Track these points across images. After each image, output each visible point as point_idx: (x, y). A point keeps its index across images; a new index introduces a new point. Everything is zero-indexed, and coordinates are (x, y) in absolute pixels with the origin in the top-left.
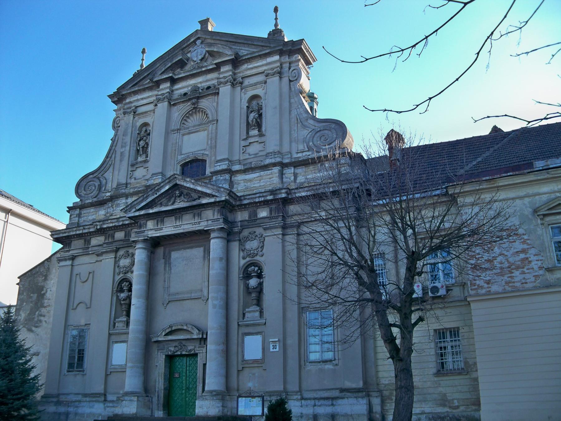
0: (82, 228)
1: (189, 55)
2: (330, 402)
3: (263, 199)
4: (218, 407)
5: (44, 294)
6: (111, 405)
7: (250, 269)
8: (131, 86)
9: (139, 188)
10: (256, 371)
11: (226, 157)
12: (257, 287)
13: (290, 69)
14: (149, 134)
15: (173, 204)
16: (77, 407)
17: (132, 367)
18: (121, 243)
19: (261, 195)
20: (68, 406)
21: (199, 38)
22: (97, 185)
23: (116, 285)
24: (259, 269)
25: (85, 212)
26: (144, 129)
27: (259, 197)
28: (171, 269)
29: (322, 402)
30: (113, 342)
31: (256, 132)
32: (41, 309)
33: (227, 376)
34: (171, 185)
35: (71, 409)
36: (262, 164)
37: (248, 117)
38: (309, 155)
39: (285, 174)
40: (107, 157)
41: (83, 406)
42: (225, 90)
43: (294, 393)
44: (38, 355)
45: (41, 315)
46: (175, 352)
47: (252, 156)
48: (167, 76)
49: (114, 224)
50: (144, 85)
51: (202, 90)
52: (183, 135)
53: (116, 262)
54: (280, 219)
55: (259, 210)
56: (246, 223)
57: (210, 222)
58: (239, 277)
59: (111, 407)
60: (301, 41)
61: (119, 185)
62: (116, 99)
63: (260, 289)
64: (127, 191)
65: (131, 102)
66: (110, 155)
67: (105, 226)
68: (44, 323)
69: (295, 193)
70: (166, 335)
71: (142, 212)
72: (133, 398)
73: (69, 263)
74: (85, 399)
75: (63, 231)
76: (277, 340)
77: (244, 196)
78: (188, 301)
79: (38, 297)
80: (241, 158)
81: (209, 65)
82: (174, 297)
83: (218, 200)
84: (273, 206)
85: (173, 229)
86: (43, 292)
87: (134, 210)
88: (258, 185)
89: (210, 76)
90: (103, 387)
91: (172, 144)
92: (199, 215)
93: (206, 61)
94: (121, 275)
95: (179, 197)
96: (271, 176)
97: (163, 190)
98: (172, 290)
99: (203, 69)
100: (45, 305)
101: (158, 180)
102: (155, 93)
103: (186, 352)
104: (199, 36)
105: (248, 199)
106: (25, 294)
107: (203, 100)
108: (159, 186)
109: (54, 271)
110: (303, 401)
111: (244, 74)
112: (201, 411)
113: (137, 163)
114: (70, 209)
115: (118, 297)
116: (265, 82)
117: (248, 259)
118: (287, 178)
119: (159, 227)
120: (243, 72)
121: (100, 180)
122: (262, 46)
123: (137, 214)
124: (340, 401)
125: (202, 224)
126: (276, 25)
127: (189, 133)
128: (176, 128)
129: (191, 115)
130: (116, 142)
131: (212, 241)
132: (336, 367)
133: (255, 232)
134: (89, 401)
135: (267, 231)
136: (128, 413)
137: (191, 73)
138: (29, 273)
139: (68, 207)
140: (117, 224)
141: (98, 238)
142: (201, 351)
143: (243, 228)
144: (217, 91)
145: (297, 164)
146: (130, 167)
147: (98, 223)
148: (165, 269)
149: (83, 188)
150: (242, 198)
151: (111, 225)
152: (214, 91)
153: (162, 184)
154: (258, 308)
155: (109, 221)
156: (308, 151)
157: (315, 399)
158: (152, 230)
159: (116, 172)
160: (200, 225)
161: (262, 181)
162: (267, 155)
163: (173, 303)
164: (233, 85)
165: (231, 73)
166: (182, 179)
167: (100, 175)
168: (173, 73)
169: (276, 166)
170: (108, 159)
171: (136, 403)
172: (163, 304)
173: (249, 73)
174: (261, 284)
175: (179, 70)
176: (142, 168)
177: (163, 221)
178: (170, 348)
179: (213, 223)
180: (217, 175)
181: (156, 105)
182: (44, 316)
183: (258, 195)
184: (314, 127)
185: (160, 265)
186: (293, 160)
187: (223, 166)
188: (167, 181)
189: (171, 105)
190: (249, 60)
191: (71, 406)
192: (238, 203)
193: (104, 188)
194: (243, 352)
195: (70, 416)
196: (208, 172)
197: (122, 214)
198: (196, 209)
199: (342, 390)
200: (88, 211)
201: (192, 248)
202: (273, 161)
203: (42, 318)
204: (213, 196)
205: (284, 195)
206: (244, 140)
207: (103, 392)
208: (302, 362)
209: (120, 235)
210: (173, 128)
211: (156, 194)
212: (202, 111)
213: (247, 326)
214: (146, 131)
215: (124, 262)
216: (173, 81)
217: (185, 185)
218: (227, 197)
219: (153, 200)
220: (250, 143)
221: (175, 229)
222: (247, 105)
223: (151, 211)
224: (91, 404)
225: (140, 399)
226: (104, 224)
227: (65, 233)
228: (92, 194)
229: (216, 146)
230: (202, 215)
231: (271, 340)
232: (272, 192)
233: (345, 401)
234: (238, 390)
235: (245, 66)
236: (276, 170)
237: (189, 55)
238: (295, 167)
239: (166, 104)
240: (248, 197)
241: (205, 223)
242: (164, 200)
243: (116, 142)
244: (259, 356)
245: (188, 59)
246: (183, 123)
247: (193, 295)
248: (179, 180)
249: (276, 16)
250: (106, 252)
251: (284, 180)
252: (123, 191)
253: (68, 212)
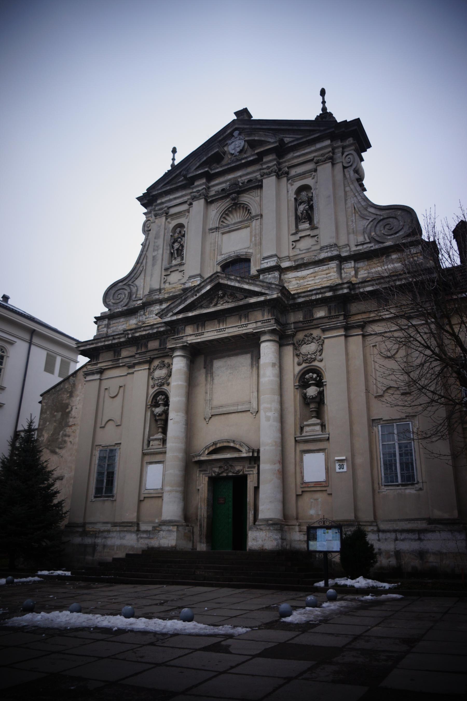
0: (111, 338)
1: (226, 149)
2: (416, 536)
3: (320, 296)
4: (276, 539)
5: (69, 412)
6: (145, 536)
7: (307, 376)
8: (161, 185)
9: (174, 292)
10: (318, 495)
11: (274, 253)
12: (316, 397)
13: (343, 154)
14: (184, 236)
15: (216, 305)
16: (105, 538)
17: (170, 491)
18: (156, 352)
19: (319, 291)
20: (96, 537)
21: (236, 129)
22: (126, 293)
23: (150, 399)
24: (318, 376)
25: (114, 322)
26: (178, 230)
27: (316, 294)
28: (213, 379)
29: (404, 535)
30: (147, 463)
31: (307, 225)
32: (65, 428)
33: (284, 502)
34: (213, 284)
35: (99, 541)
36: (317, 259)
37: (296, 210)
38: (371, 247)
39: (344, 269)
40: (137, 263)
41: (112, 537)
42: (270, 183)
43: (368, 524)
44: (62, 479)
45: (66, 435)
46: (220, 474)
47: (304, 251)
48: (202, 171)
49: (147, 332)
50: (176, 183)
51: (242, 183)
52: (223, 234)
53: (150, 374)
54: (341, 318)
55: (315, 310)
56: (300, 325)
57: (259, 324)
58: (295, 386)
59: (146, 538)
60: (357, 122)
61: (152, 291)
62: (146, 201)
63: (320, 400)
64: (161, 297)
65: (162, 203)
66: (141, 261)
67: (137, 335)
68: (69, 443)
69: (359, 288)
70: (210, 453)
71: (180, 316)
72: (171, 528)
73: (97, 377)
74: (114, 529)
75: (90, 342)
76: (344, 458)
77: (298, 294)
78: (233, 415)
79: (62, 415)
80: (291, 255)
81: (250, 157)
82: (218, 410)
83: (268, 297)
84: (333, 305)
85: (216, 334)
86: (67, 410)
87: (171, 314)
88: (313, 282)
89: (250, 169)
90: (135, 514)
91: (211, 244)
92: (246, 317)
93: (245, 153)
94: (156, 388)
95: (222, 298)
96: (327, 271)
97: (204, 291)
98: (216, 403)
99: (243, 161)
100: (70, 424)
101: (197, 281)
102: (190, 191)
103: (233, 473)
104: (236, 126)
105: (303, 297)
106: (48, 413)
107: (245, 195)
108: (200, 287)
110: (381, 534)
111: (290, 163)
112: (255, 544)
113: (171, 267)
114: (98, 320)
115: (152, 412)
116: (315, 170)
117: (304, 365)
118: (346, 273)
119: (200, 331)
120: (289, 160)
121: (130, 288)
122: (310, 131)
123: (175, 318)
124: (429, 535)
125: (250, 326)
126: (324, 109)
127: (229, 232)
128: (214, 226)
129: (231, 212)
130: (146, 247)
131: (263, 346)
132: (421, 492)
133: (311, 334)
134: (120, 531)
135: (326, 333)
136: (166, 545)
137: (229, 166)
138: (53, 390)
139: (95, 318)
140: (151, 332)
141: (129, 349)
142: (251, 472)
143: (298, 330)
144: (260, 183)
145: (357, 257)
146: (163, 271)
147: (129, 332)
148: (206, 380)
149: (111, 297)
150: (296, 296)
151: (144, 333)
152: (257, 184)
153: (203, 284)
154: (318, 421)
155: (142, 329)
156: (370, 243)
157: (395, 531)
158: (191, 336)
159: (148, 278)
160: (248, 327)
161: (317, 278)
162: (322, 249)
163: (217, 417)
164: (279, 177)
165: (275, 162)
166: (225, 277)
167: (130, 283)
168: (209, 168)
169: (333, 260)
170: (139, 265)
171: (175, 534)
172: (205, 419)
173: (296, 161)
174: (321, 394)
175: (214, 165)
176: (177, 272)
177: (203, 326)
178: (214, 469)
179: (263, 324)
180: (264, 273)
181: (191, 204)
182: (69, 436)
183: (314, 292)
184: (375, 216)
185: (201, 376)
186: (352, 253)
187: (272, 263)
188: (208, 281)
189: (209, 202)
191: (98, 537)
192: (291, 302)
193: (134, 296)
194: (302, 473)
195: (98, 548)
196: (253, 271)
197: (159, 320)
198: (242, 311)
199: (430, 521)
200: (118, 321)
201: (236, 355)
202: (329, 254)
203: (67, 438)
204: (261, 294)
205: (345, 291)
206: (293, 234)
207: (135, 520)
208: (376, 486)
209: (153, 345)
210: (211, 226)
211: (196, 295)
212: (243, 207)
213: (306, 441)
214: (180, 232)
215: (160, 373)
216: (210, 177)
217: (229, 283)
218: (279, 295)
219: (193, 302)
220: (301, 237)
221: (218, 333)
222: (295, 196)
223: (190, 314)
224: (122, 534)
225: (180, 528)
226: (136, 332)
227: (92, 344)
228: (122, 303)
229: (261, 244)
230: (250, 317)
231: (336, 458)
232: (331, 288)
233: (437, 535)
234: (297, 519)
235: (291, 155)
236: (333, 265)
237: (226, 149)
238: (355, 261)
239: (202, 201)
240: (303, 295)
241: (254, 325)
242: (204, 302)
243: (146, 247)
244: (321, 477)
245: (225, 153)
246: (223, 222)
247: (240, 407)
248: (222, 279)
249: (323, 99)
250: (139, 363)
251: (344, 275)
252: (157, 297)
253: (96, 323)
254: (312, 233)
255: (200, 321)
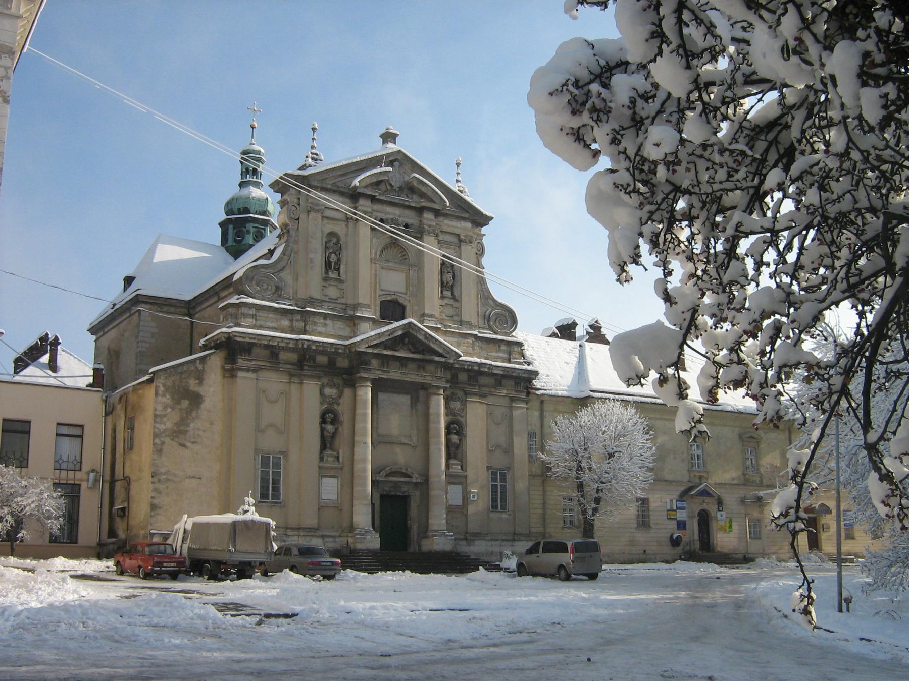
31: (448, 293)
70: (388, 475)
109: (213, 376)
116: (459, 247)
123: (370, 350)
173: (446, 229)
190: (446, 216)
244: (460, 502)
254: (456, 305)
255: (386, 360)
